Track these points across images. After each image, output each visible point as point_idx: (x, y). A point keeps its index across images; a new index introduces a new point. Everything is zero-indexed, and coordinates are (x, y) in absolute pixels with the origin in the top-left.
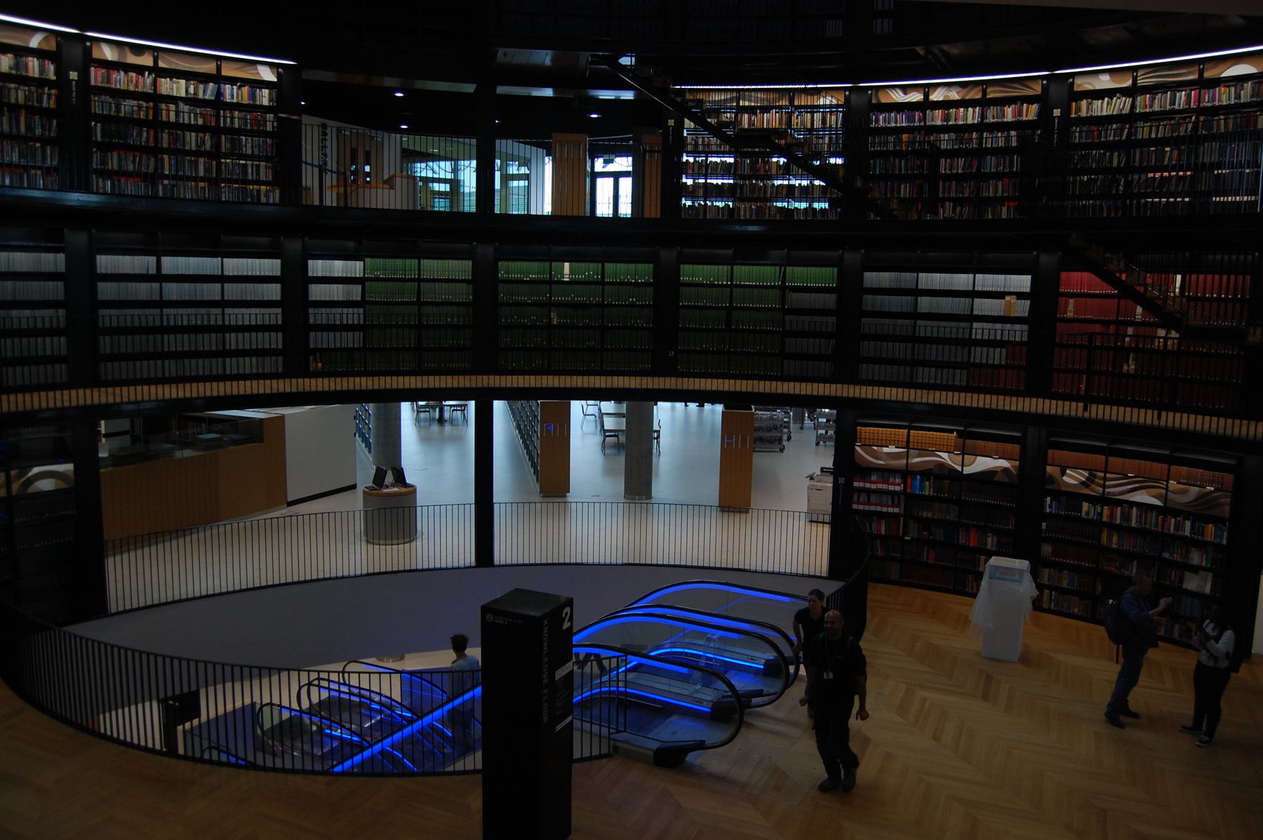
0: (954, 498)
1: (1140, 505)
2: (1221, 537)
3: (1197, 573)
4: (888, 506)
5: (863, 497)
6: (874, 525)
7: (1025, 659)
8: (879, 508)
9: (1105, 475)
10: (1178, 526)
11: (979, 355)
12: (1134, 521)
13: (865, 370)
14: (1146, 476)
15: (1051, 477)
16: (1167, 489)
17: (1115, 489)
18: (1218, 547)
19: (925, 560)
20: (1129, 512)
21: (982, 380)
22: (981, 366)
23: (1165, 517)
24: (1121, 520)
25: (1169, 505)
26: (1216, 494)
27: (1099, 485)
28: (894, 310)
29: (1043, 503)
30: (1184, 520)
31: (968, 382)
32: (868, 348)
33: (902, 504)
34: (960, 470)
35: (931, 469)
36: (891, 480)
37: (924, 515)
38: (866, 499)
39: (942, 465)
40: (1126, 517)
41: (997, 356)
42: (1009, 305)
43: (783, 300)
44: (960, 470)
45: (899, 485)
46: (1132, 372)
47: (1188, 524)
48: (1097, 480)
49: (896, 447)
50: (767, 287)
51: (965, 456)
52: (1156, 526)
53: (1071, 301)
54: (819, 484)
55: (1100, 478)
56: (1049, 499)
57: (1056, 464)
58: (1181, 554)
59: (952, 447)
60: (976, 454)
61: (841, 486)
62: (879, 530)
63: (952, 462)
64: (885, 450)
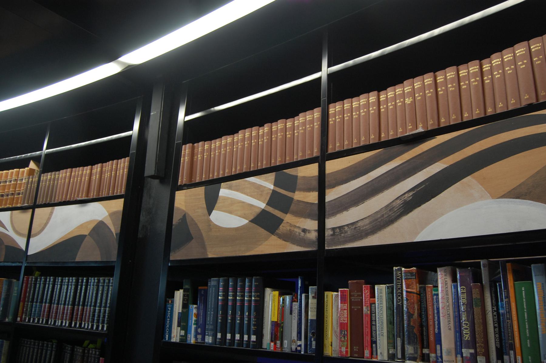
9: (322, 169)
20: (421, 297)
24: (392, 343)
34: (24, 248)
44: (24, 248)
48: (298, 196)
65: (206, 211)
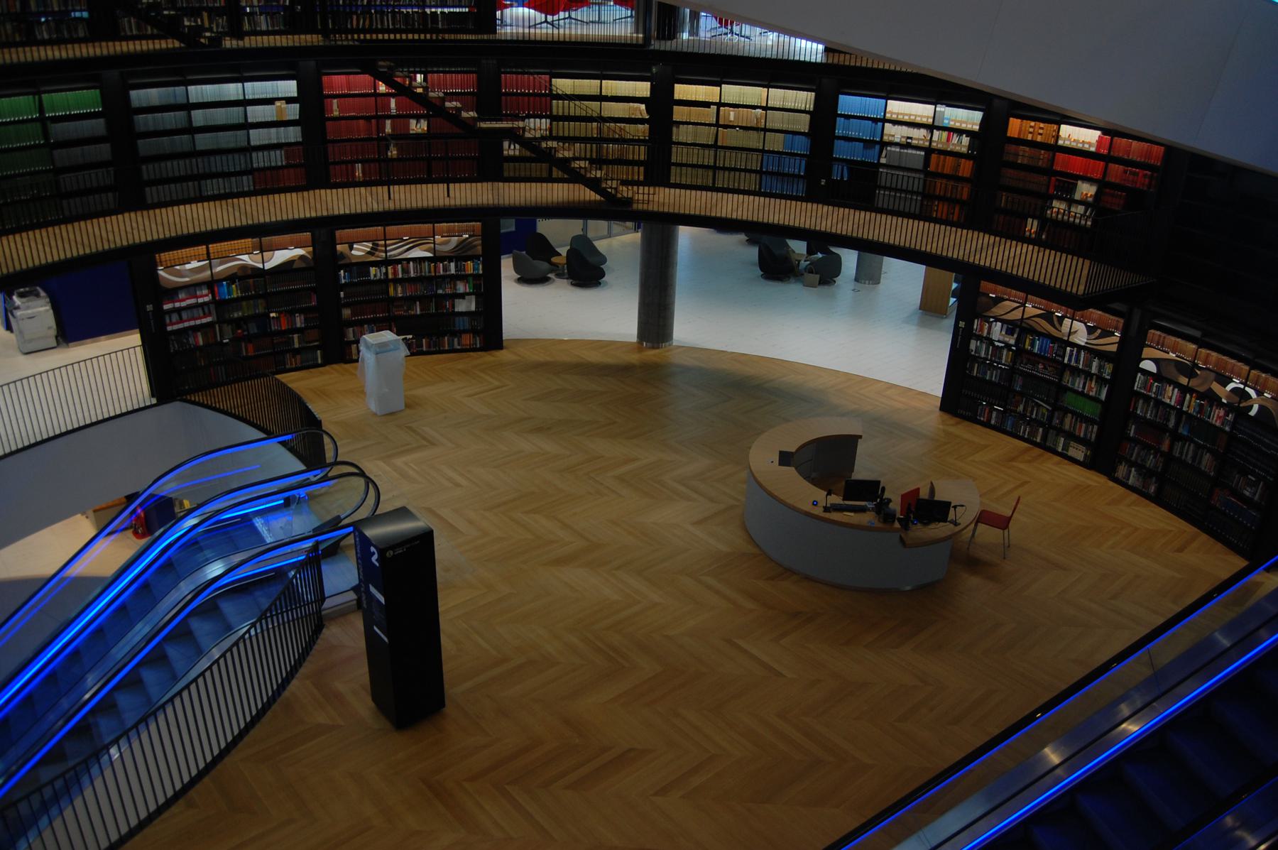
0: (261, 292)
1: (414, 260)
2: (478, 269)
3: (464, 298)
4: (200, 318)
5: (175, 317)
6: (191, 340)
7: (408, 406)
8: (192, 323)
10: (445, 269)
11: (259, 160)
12: (412, 272)
13: (151, 193)
14: (417, 236)
15: (341, 253)
16: (434, 243)
17: (395, 251)
18: (476, 277)
19: (245, 354)
21: (268, 184)
22: (264, 169)
23: (436, 263)
24: (402, 274)
25: (437, 255)
26: (470, 240)
27: (382, 251)
28: (169, 127)
29: (338, 277)
30: (449, 263)
31: (254, 187)
32: (148, 171)
33: (214, 312)
35: (236, 273)
36: (198, 293)
37: (236, 315)
38: (178, 318)
39: (244, 267)
40: (405, 271)
41: (277, 158)
42: (280, 110)
43: (46, 134)
45: (206, 295)
46: (395, 157)
47: (453, 265)
48: (379, 248)
49: (199, 261)
50: (23, 122)
51: (264, 253)
52: (430, 272)
53: (335, 101)
54: (29, 311)
55: (382, 246)
56: (342, 271)
57: (344, 242)
58: (451, 288)
59: (251, 249)
60: (273, 248)
61: (150, 313)
62: (197, 342)
63: (252, 261)
64: (188, 266)
65: (348, 249)
